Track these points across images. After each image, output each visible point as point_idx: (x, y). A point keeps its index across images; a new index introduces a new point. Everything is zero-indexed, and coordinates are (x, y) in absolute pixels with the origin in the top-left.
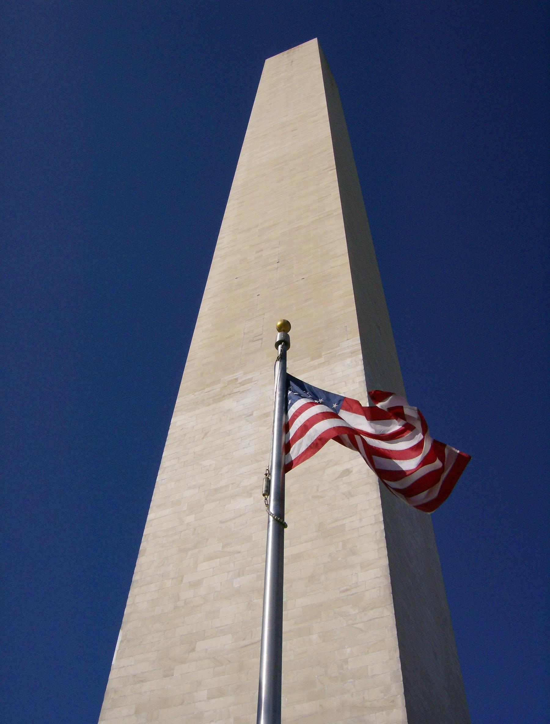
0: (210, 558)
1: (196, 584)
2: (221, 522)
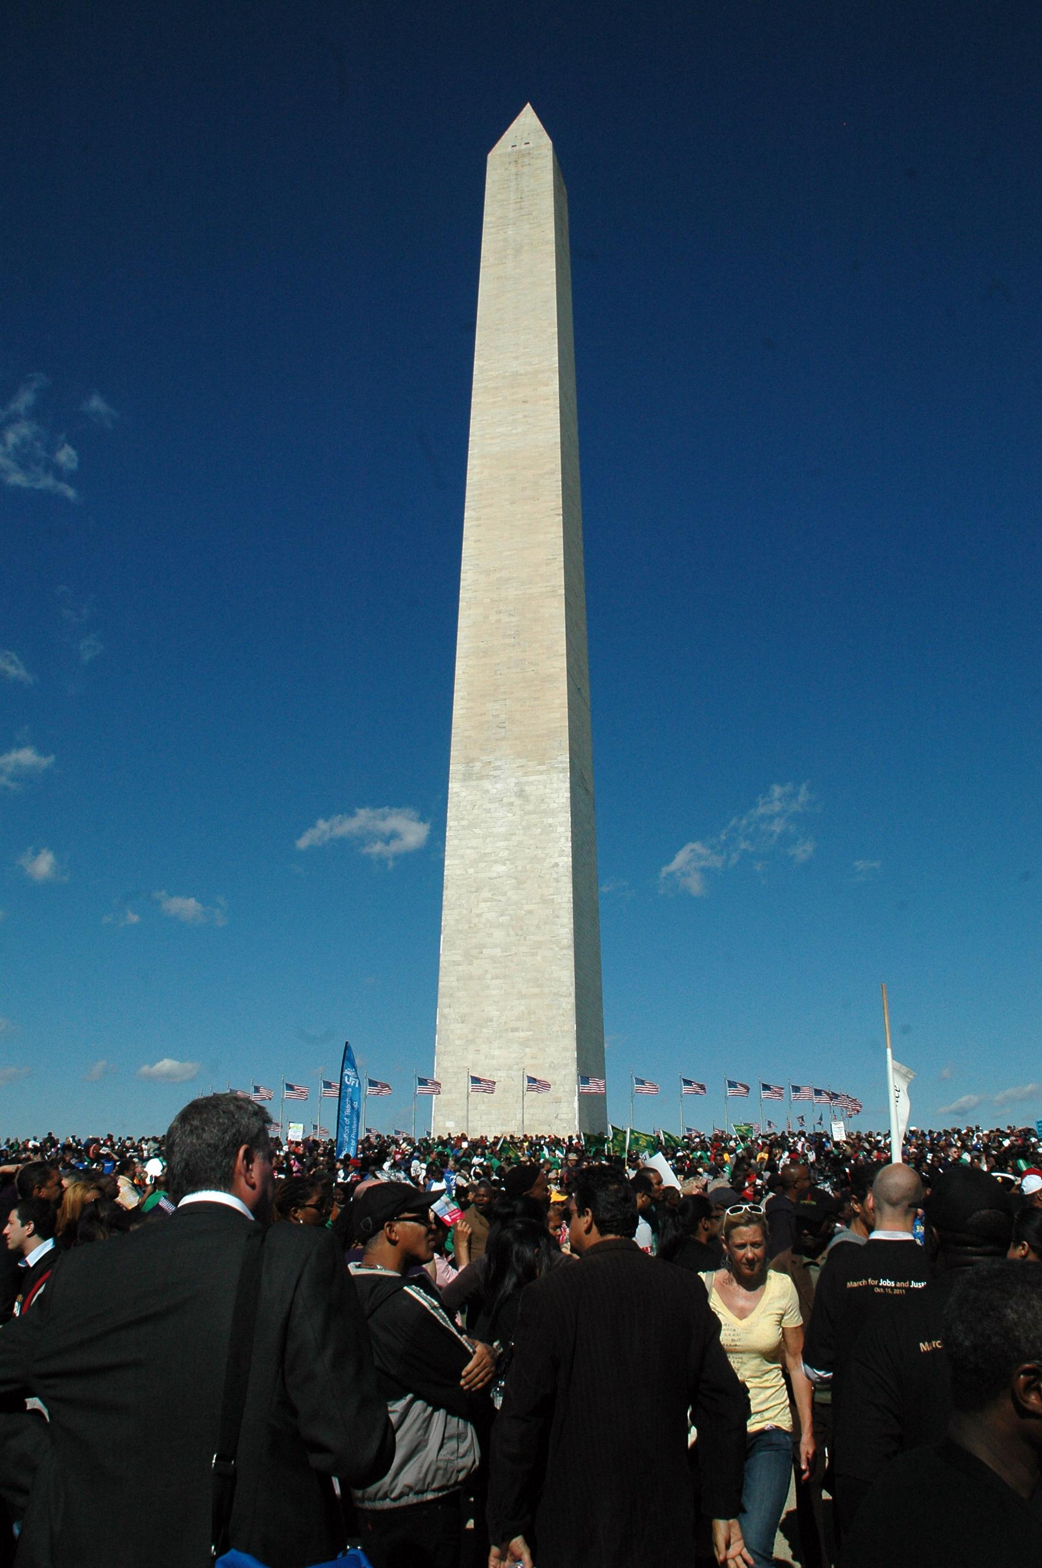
0: (485, 901)
1: (479, 915)
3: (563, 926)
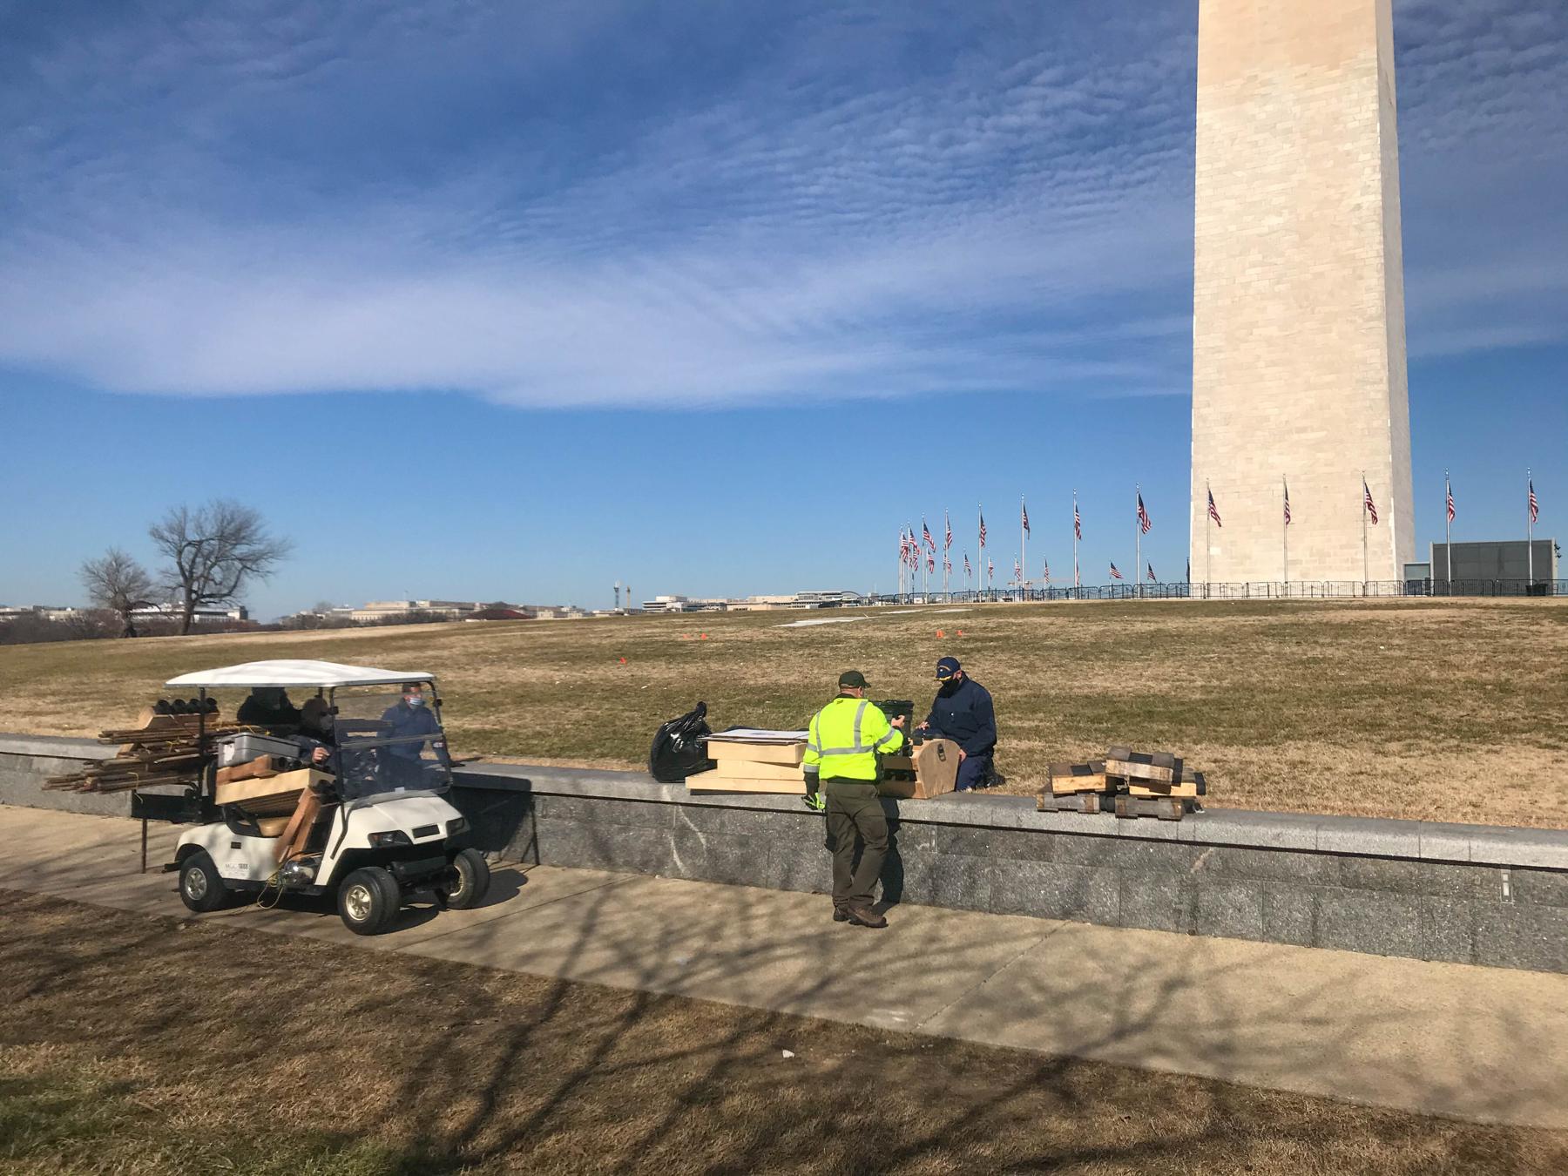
1: (1246, 285)
2: (1260, 236)
3: (1369, 290)
